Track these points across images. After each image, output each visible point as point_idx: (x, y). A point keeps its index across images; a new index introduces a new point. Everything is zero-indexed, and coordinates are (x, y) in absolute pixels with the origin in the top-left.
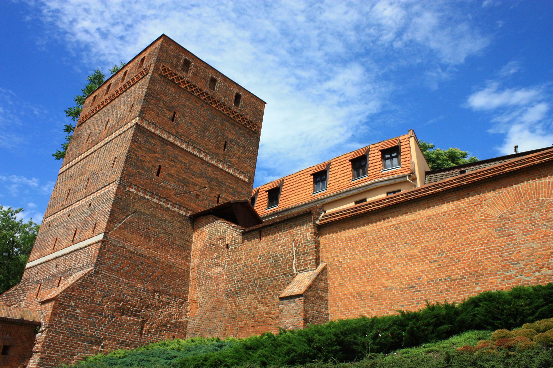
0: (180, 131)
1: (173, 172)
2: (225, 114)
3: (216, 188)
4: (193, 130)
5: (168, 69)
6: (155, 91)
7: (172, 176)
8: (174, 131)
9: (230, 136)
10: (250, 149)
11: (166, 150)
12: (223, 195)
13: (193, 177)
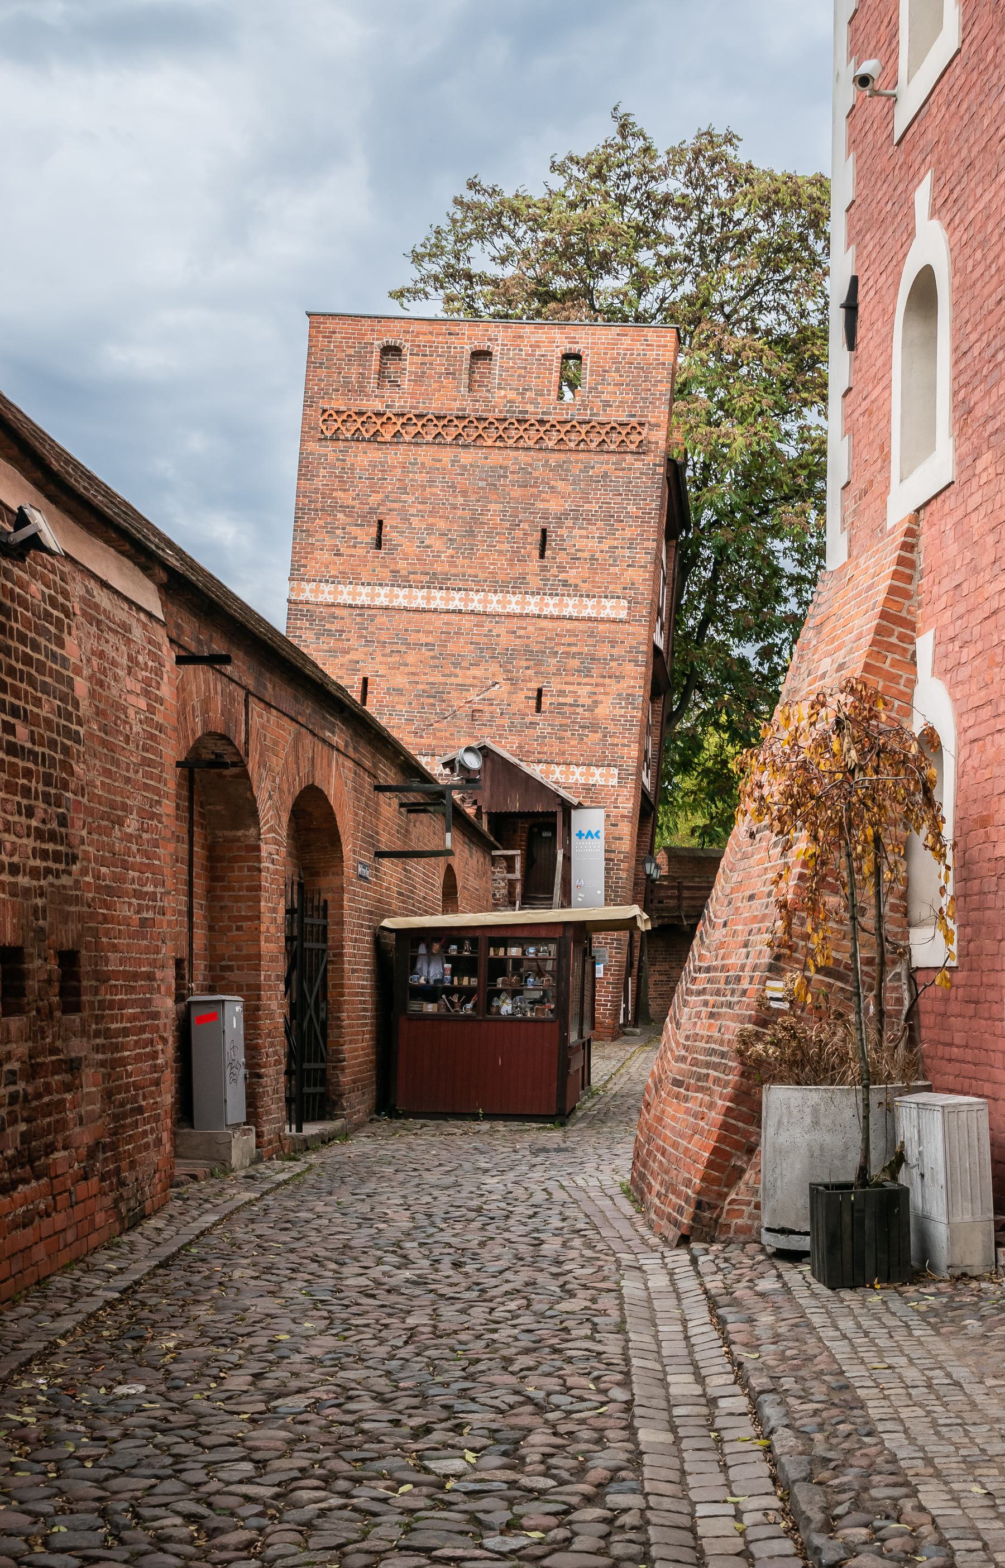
0: (402, 565)
1: (400, 680)
2: (529, 449)
3: (530, 672)
4: (438, 544)
5: (338, 412)
6: (316, 491)
7: (400, 692)
8: (386, 573)
9: (554, 506)
11: (373, 633)
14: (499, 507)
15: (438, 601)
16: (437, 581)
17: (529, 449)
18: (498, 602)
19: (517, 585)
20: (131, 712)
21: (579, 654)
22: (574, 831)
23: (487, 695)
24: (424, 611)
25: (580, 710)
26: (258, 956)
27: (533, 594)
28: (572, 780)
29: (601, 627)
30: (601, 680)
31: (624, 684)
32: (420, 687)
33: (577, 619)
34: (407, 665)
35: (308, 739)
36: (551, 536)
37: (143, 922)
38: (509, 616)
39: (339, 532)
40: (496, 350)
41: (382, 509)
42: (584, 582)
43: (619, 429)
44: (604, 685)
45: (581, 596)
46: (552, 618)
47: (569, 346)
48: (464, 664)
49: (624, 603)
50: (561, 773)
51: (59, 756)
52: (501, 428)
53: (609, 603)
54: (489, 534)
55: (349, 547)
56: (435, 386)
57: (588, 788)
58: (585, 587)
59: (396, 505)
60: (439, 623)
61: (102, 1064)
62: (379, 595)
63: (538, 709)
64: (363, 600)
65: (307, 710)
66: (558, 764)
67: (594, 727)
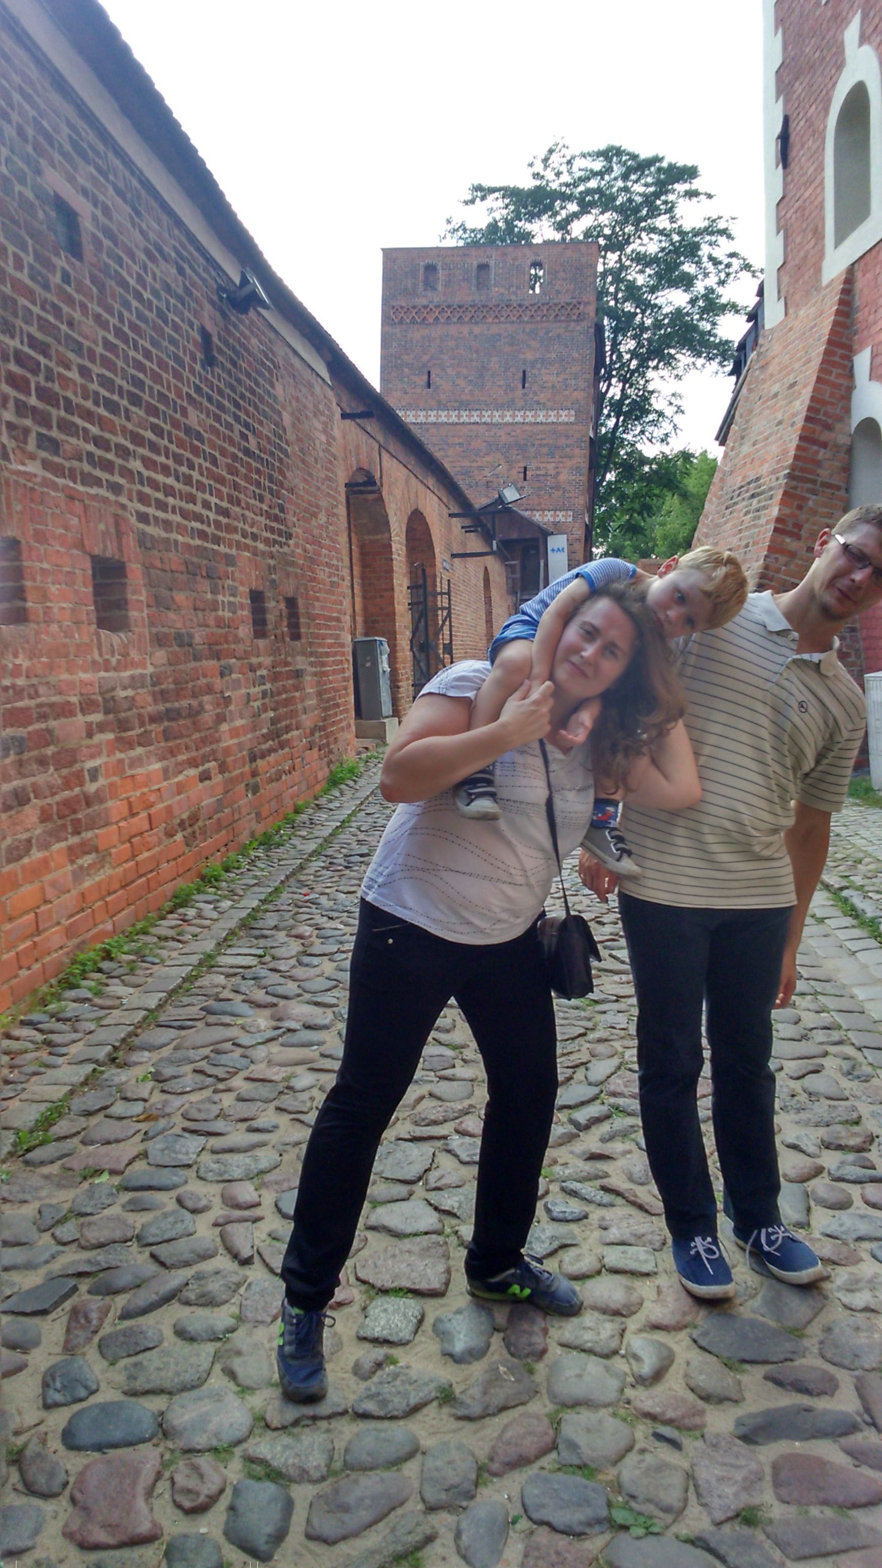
0: (443, 397)
4: (461, 382)
5: (402, 307)
9: (529, 356)
10: (573, 359)
12: (532, 466)
13: (478, 459)
14: (497, 359)
16: (463, 405)
19: (510, 405)
20: (317, 442)
26: (394, 614)
28: (546, 519)
29: (560, 428)
31: (574, 461)
35: (413, 480)
36: (528, 375)
37: (333, 584)
38: (507, 424)
40: (492, 263)
41: (430, 364)
46: (531, 424)
49: (573, 412)
51: (277, 464)
53: (563, 413)
57: (555, 524)
58: (549, 404)
61: (315, 674)
63: (525, 479)
65: (412, 462)
67: (557, 487)
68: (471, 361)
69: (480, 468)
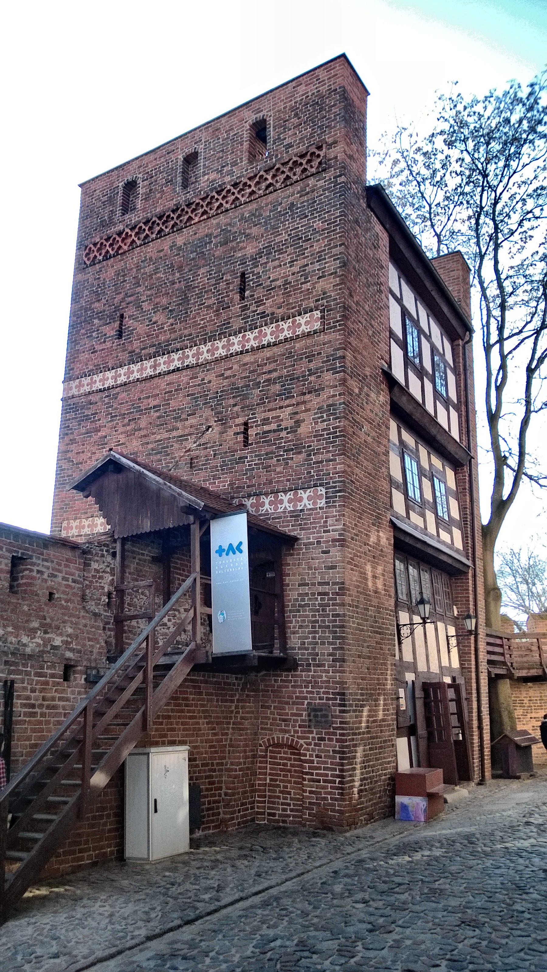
2: (227, 210)
5: (95, 244)
9: (250, 250)
11: (116, 409)
13: (179, 425)
15: (162, 366)
17: (227, 210)
18: (208, 351)
21: (279, 378)
22: (214, 547)
23: (202, 441)
24: (152, 377)
25: (283, 434)
27: (235, 334)
29: (298, 345)
30: (302, 398)
32: (150, 446)
33: (275, 344)
34: (140, 429)
39: (94, 334)
40: (201, 148)
41: (124, 305)
42: (279, 308)
43: (300, 161)
44: (304, 402)
45: (277, 321)
47: (255, 117)
48: (184, 416)
50: (271, 503)
52: (205, 204)
53: (301, 320)
54: (199, 296)
55: (101, 343)
56: (158, 195)
57: (296, 515)
59: (132, 298)
60: (163, 386)
62: (120, 375)
63: (246, 443)
64: (110, 383)
66: (266, 494)
68: (173, 283)
69: (182, 438)
